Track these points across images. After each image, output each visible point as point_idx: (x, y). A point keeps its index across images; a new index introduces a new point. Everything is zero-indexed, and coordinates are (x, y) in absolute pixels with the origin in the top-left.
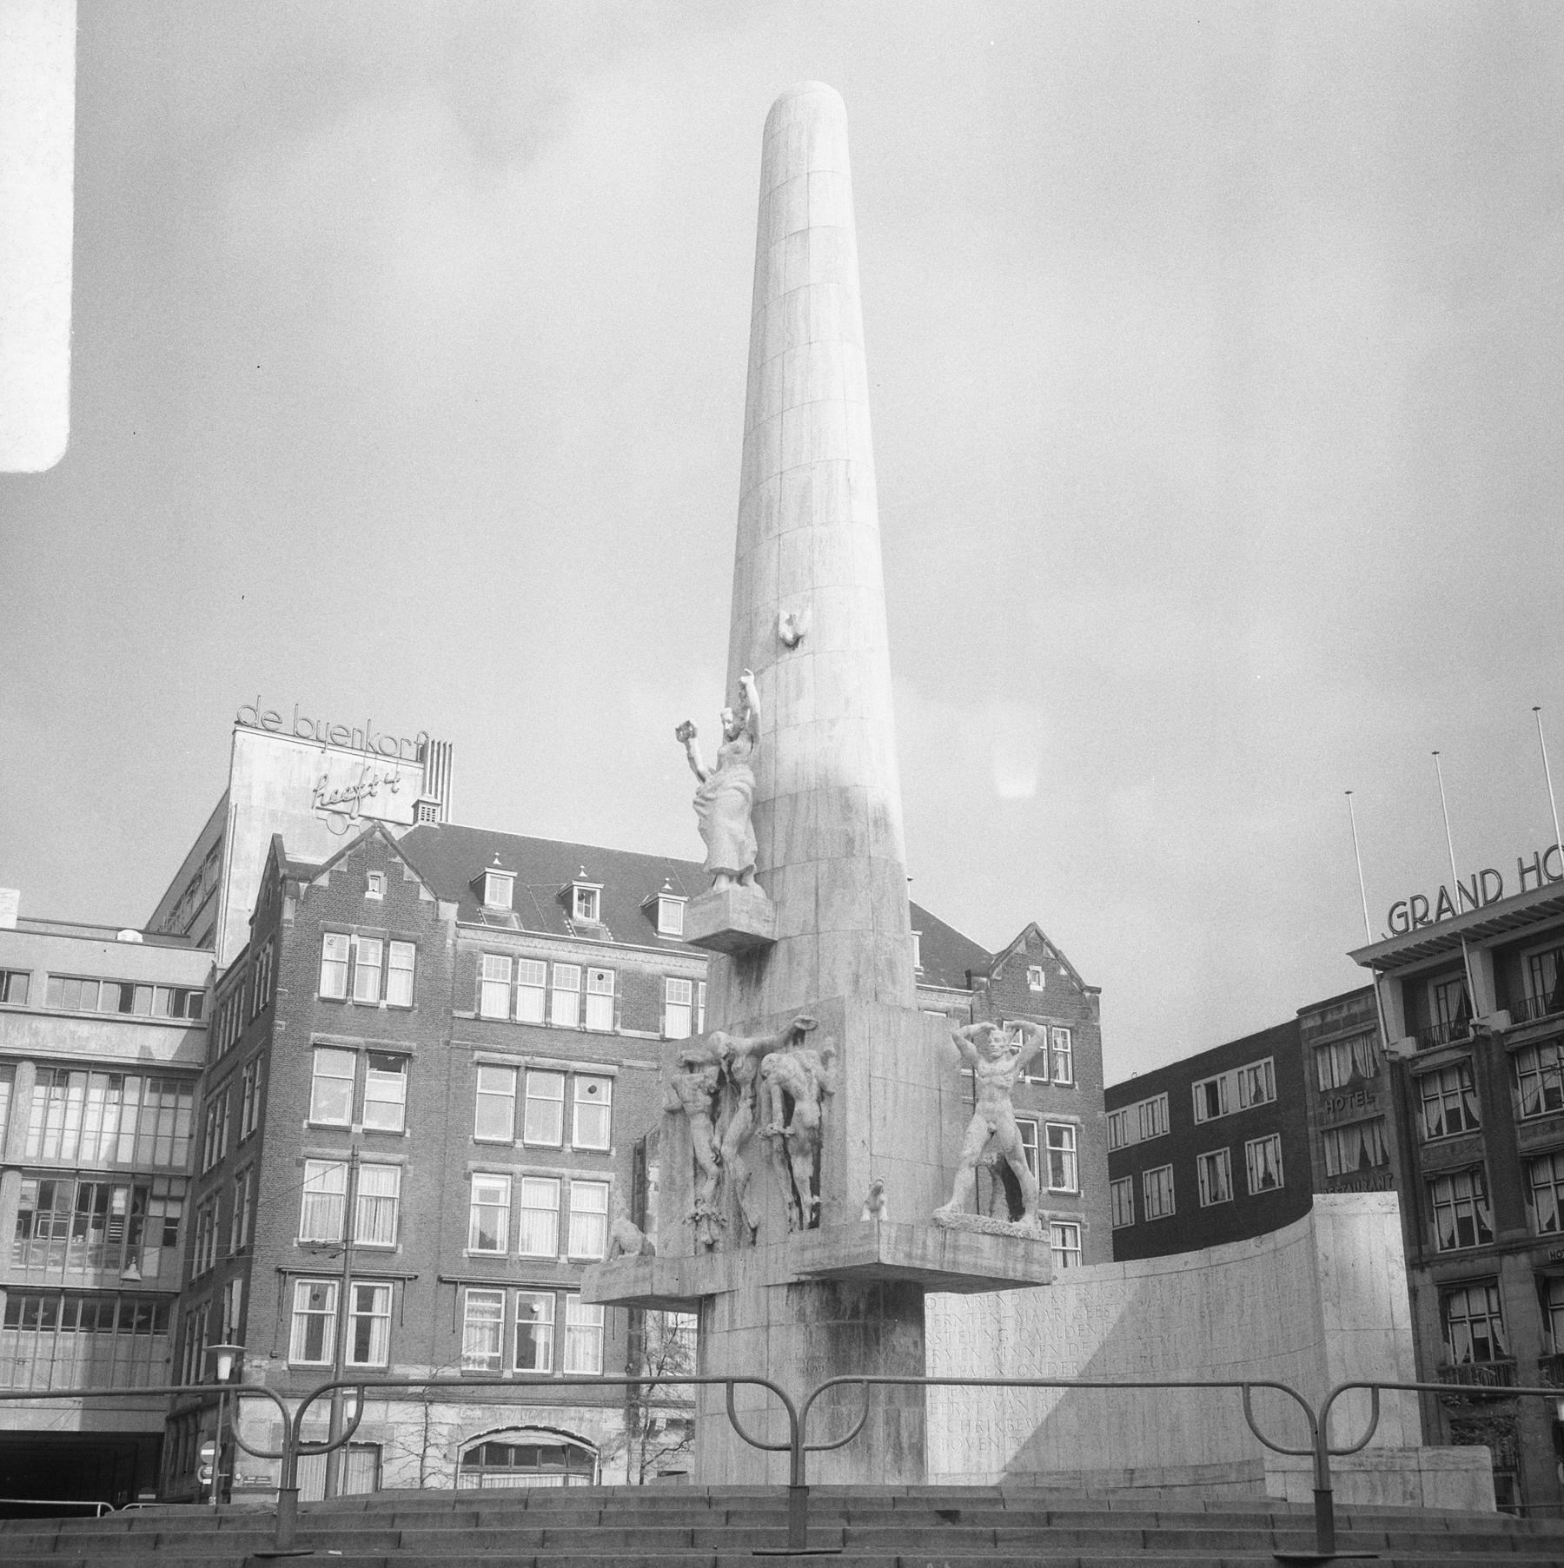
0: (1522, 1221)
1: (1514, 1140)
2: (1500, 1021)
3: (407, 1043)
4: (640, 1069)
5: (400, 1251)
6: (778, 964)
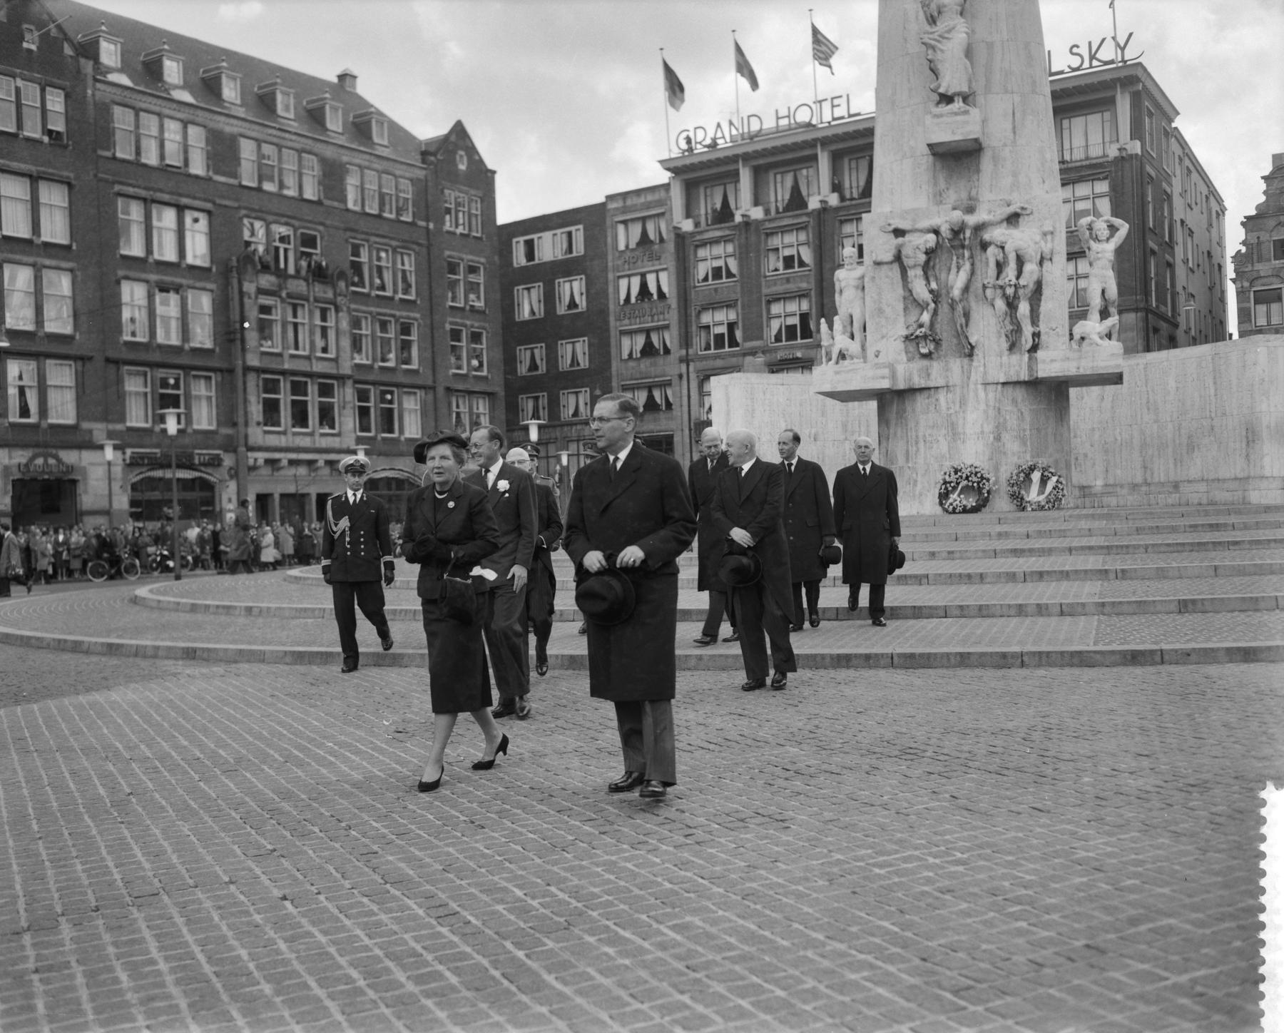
0: (761, 338)
1: (759, 286)
2: (757, 213)
3: (65, 174)
4: (226, 206)
6: (986, 163)
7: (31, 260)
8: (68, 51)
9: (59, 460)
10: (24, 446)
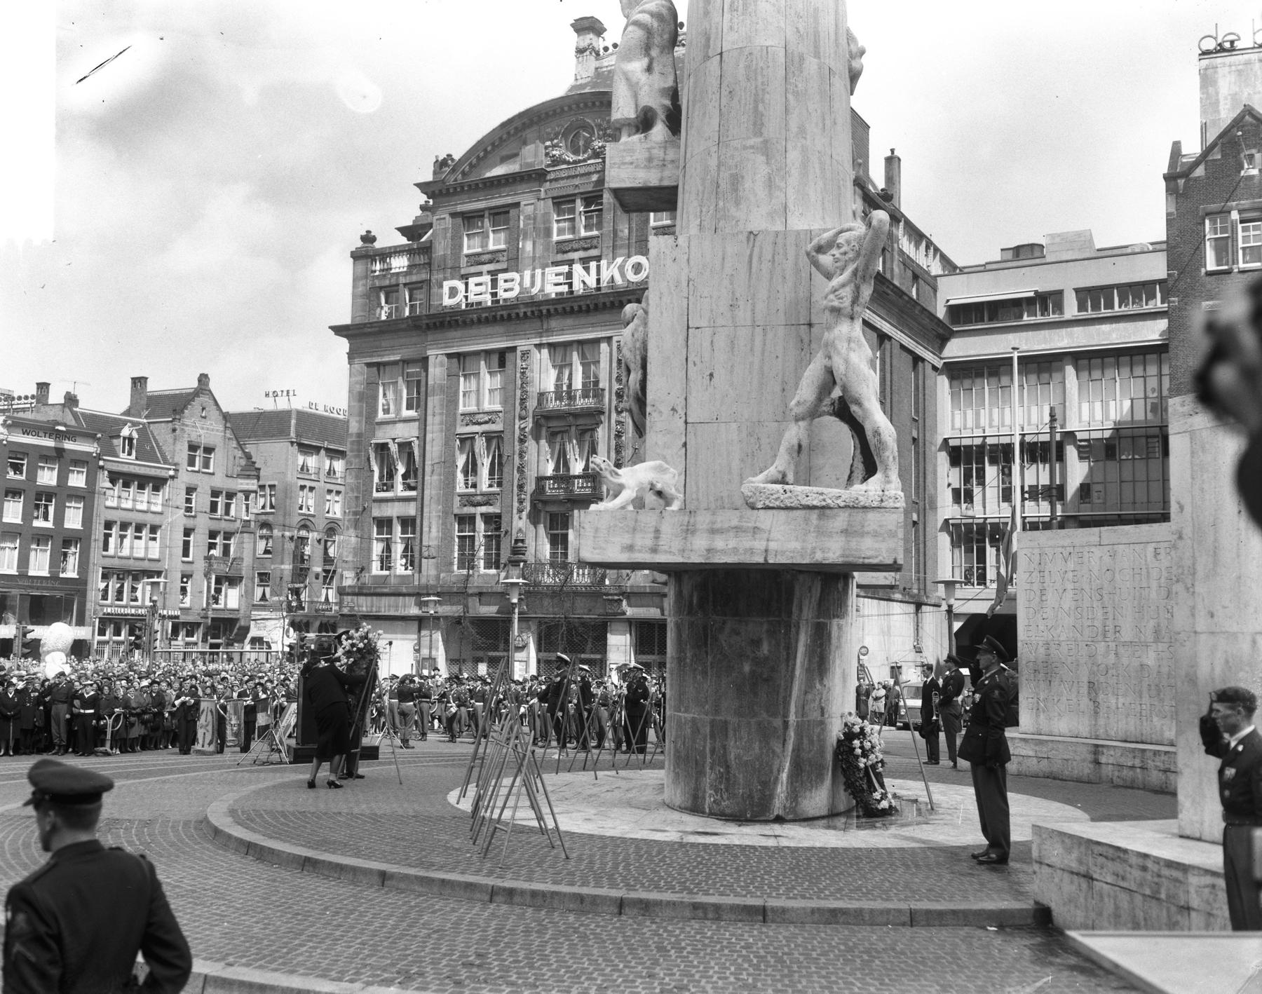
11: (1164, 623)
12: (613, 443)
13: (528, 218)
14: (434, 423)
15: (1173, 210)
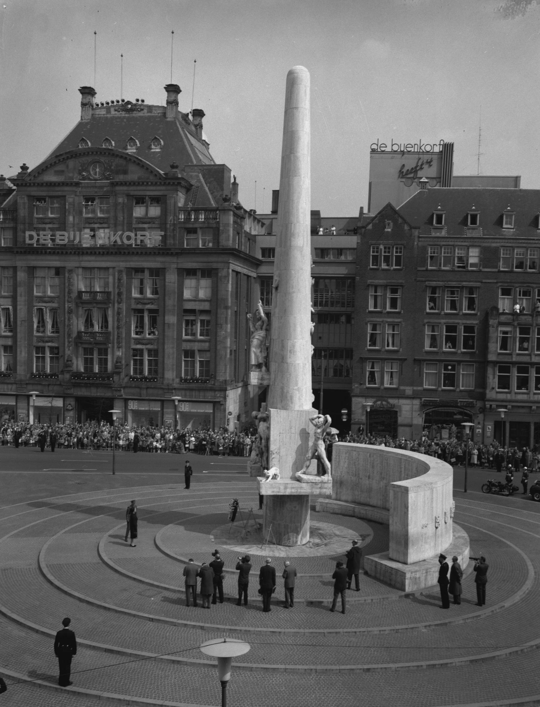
3: (400, 281)
5: (401, 350)
7: (381, 320)
8: (406, 227)
9: (388, 403)
10: (372, 397)
11: (371, 475)
12: (116, 318)
13: (70, 204)
14: (21, 300)
15: (359, 241)
